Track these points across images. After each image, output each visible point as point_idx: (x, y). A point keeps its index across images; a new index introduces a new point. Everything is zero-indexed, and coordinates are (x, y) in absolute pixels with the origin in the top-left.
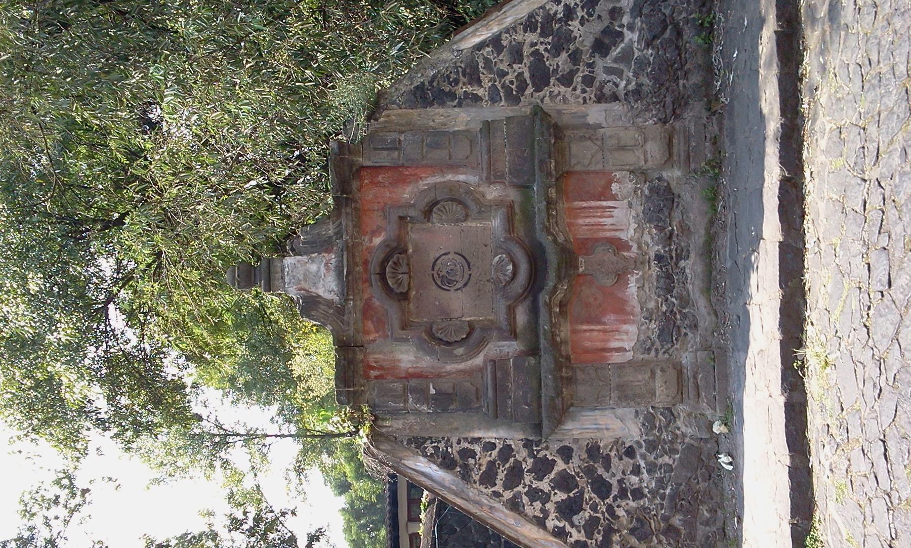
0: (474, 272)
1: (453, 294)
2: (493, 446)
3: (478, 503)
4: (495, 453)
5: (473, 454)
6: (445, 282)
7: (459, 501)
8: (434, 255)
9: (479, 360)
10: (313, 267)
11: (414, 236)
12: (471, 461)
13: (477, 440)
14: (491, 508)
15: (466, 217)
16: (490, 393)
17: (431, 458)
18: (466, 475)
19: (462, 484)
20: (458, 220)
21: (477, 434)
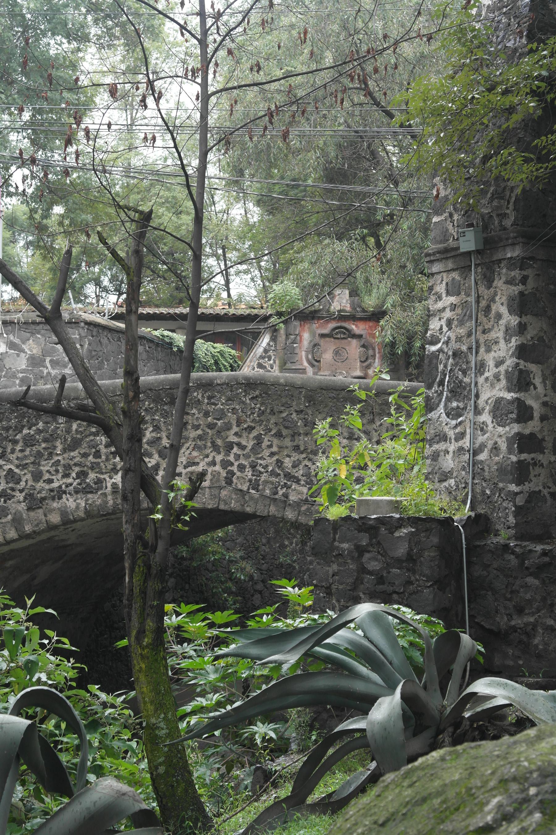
0: (340, 364)
1: (332, 355)
2: (272, 368)
3: (251, 362)
4: (269, 369)
5: (269, 360)
6: (337, 353)
7: (252, 354)
8: (347, 348)
9: (306, 364)
10: (344, 301)
11: (354, 342)
12: (267, 359)
13: (275, 362)
14: (249, 366)
15: (361, 361)
16: (294, 367)
17: (268, 344)
18: (262, 357)
19: (258, 356)
20: (360, 358)
21: (277, 362)
